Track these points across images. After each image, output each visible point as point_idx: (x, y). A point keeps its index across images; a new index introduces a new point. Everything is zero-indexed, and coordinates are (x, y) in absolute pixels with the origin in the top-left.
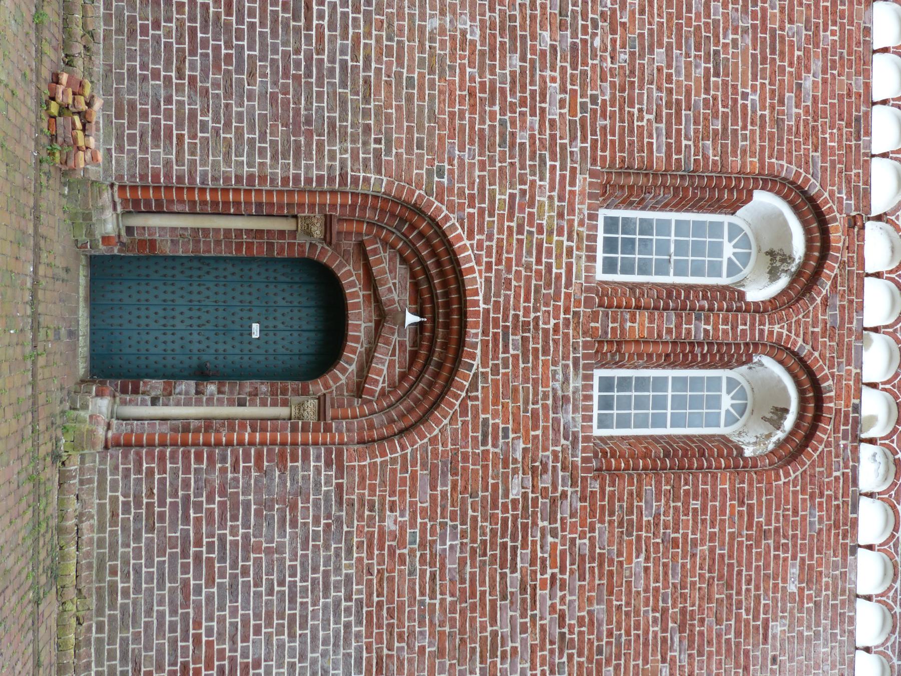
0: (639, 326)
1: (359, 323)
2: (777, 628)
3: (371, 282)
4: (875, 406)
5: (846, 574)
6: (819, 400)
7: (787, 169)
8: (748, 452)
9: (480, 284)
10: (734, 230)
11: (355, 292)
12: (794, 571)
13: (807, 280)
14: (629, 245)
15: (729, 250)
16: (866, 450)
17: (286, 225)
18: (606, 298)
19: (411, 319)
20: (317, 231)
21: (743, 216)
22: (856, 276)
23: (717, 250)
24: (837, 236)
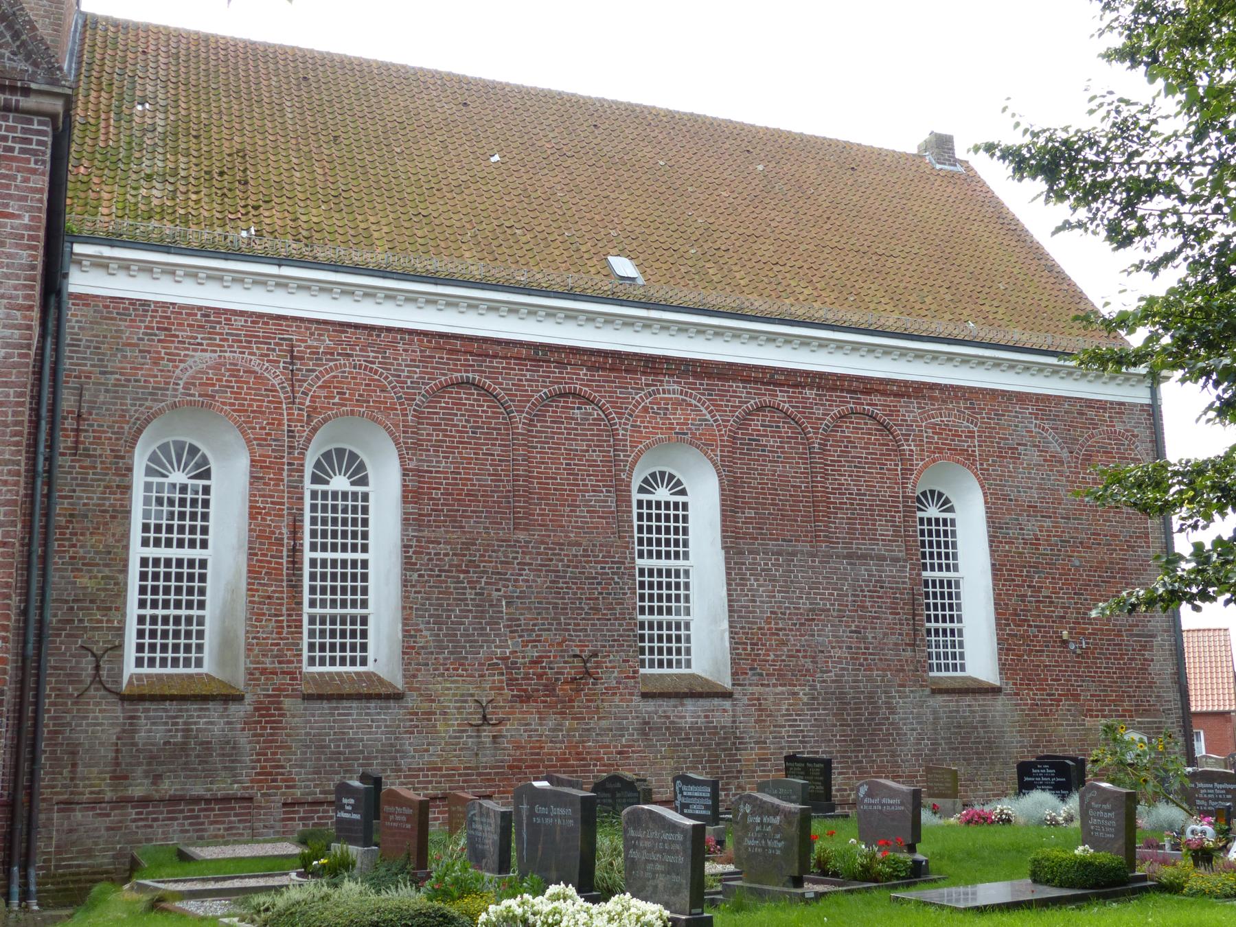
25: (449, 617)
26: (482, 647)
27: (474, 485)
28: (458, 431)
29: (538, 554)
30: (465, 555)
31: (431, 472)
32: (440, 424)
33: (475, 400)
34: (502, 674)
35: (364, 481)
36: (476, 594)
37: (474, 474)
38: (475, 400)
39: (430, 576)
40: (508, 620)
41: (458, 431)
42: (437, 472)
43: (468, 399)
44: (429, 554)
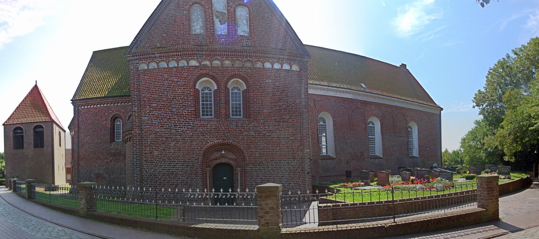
0: (223, 111)
1: (224, 160)
2: (277, 84)
3: (216, 159)
4: (237, 64)
5: (268, 69)
6: (236, 75)
7: (192, 83)
8: (245, 88)
9: (217, 141)
10: (203, 90)
11: (218, 161)
12: (267, 81)
13: (213, 78)
14: (207, 111)
15: (206, 91)
16: (245, 66)
17: (208, 173)
18: (218, 116)
19: (223, 152)
20: (208, 169)
21: (200, 90)
22: (213, 68)
23: (207, 93)
24: (204, 72)
35: (325, 123)
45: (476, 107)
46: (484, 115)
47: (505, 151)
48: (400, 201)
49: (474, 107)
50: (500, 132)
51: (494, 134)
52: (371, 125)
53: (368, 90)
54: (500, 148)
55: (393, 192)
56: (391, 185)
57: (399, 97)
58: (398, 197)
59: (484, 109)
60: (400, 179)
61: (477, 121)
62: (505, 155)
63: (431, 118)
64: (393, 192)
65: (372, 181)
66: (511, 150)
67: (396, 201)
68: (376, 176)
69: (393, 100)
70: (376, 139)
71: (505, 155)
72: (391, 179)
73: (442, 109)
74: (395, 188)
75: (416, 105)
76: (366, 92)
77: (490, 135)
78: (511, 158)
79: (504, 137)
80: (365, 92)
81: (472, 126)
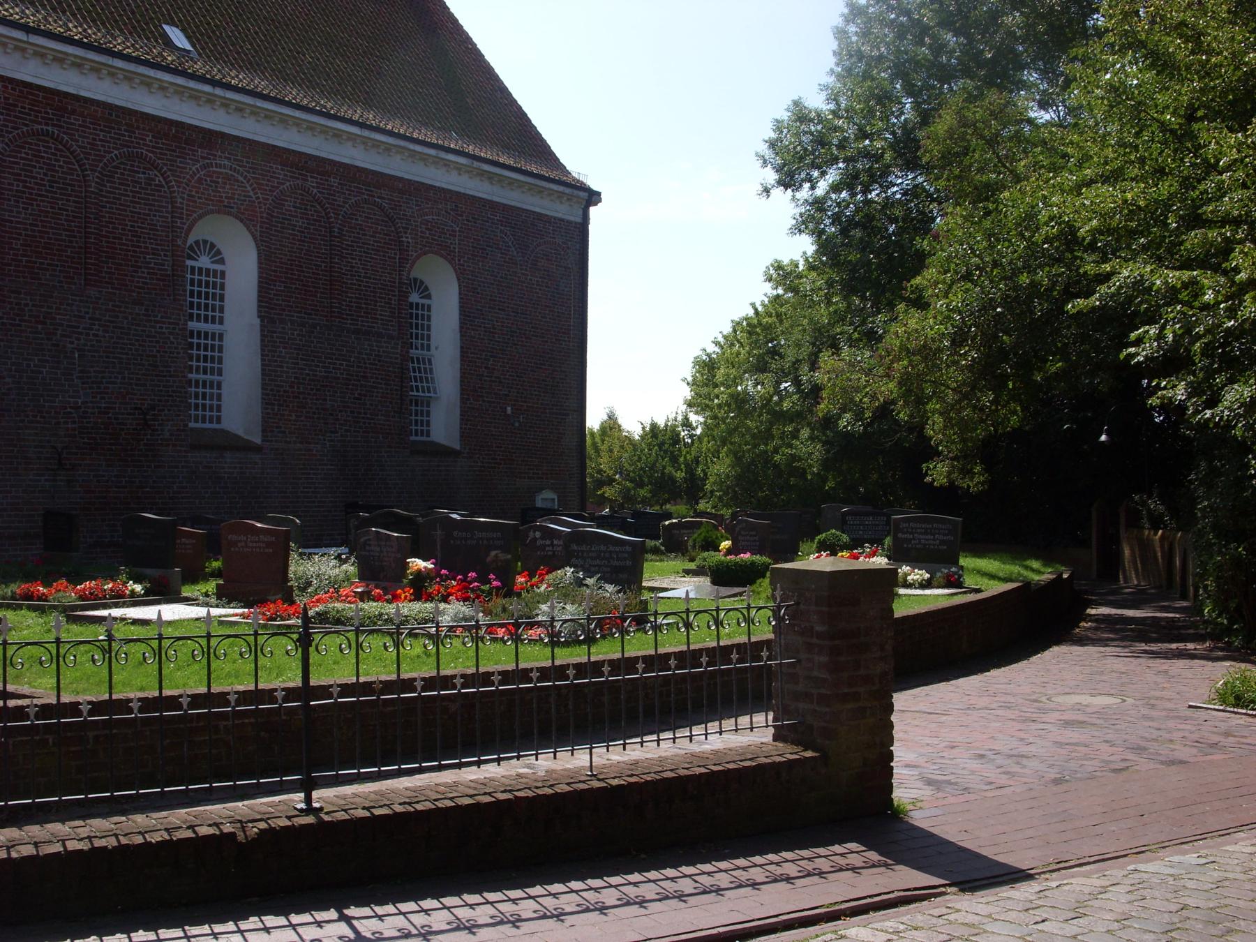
25: (28, 366)
26: (57, 396)
27: (50, 239)
28: (36, 184)
29: (106, 310)
30: (42, 306)
31: (11, 222)
32: (20, 175)
33: (53, 154)
34: (74, 422)
36: (53, 345)
37: (52, 228)
38: (53, 154)
39: (12, 325)
40: (81, 372)
41: (36, 184)
42: (18, 223)
43: (46, 152)
44: (11, 303)
45: (777, 192)
46: (818, 234)
47: (935, 427)
48: (346, 689)
49: (767, 191)
50: (908, 326)
51: (872, 338)
52: (204, 262)
53: (199, 67)
54: (903, 416)
55: (305, 642)
56: (301, 601)
57: (371, 117)
58: (335, 666)
59: (818, 204)
60: (350, 568)
61: (779, 267)
62: (931, 453)
63: (532, 247)
64: (305, 642)
65: (194, 577)
66: (964, 426)
67: (324, 691)
68: (213, 546)
69: (337, 135)
70: (227, 341)
71: (931, 453)
72: (299, 567)
73: (593, 197)
74: (323, 617)
75: (459, 168)
76: (193, 77)
77: (852, 343)
78: (966, 472)
79: (927, 353)
80: (183, 74)
81: (751, 293)
